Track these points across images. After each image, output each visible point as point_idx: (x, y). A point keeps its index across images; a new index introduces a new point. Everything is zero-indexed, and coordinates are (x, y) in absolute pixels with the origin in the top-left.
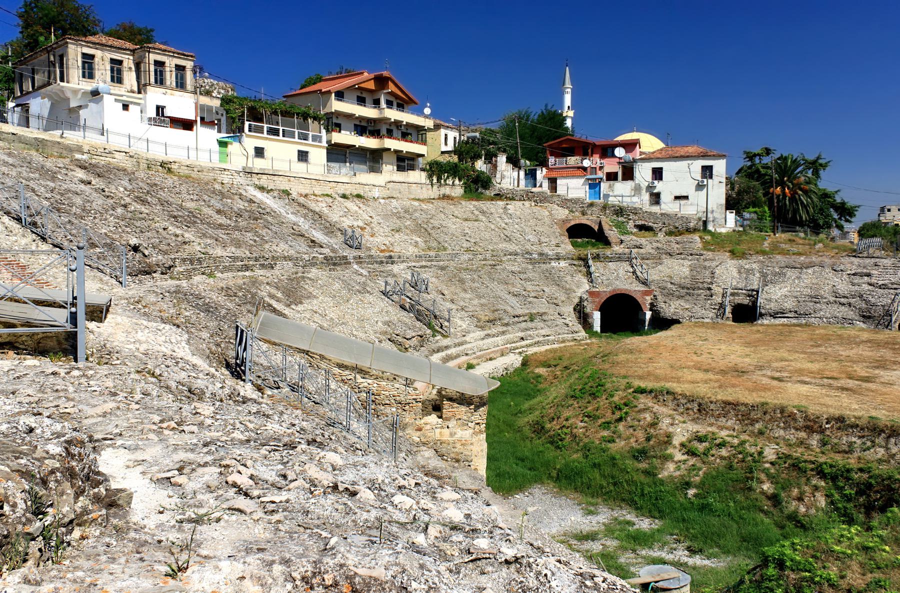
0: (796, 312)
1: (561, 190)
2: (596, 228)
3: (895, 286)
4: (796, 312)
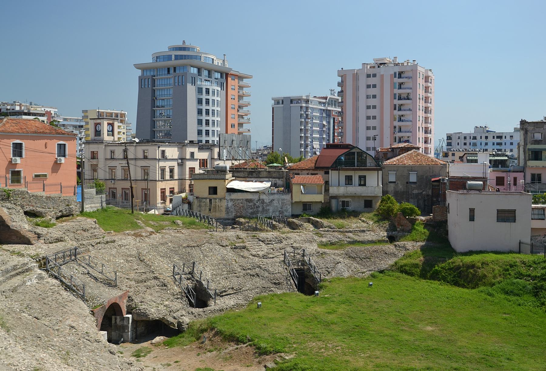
0: (233, 288)
3: (271, 256)
4: (233, 288)
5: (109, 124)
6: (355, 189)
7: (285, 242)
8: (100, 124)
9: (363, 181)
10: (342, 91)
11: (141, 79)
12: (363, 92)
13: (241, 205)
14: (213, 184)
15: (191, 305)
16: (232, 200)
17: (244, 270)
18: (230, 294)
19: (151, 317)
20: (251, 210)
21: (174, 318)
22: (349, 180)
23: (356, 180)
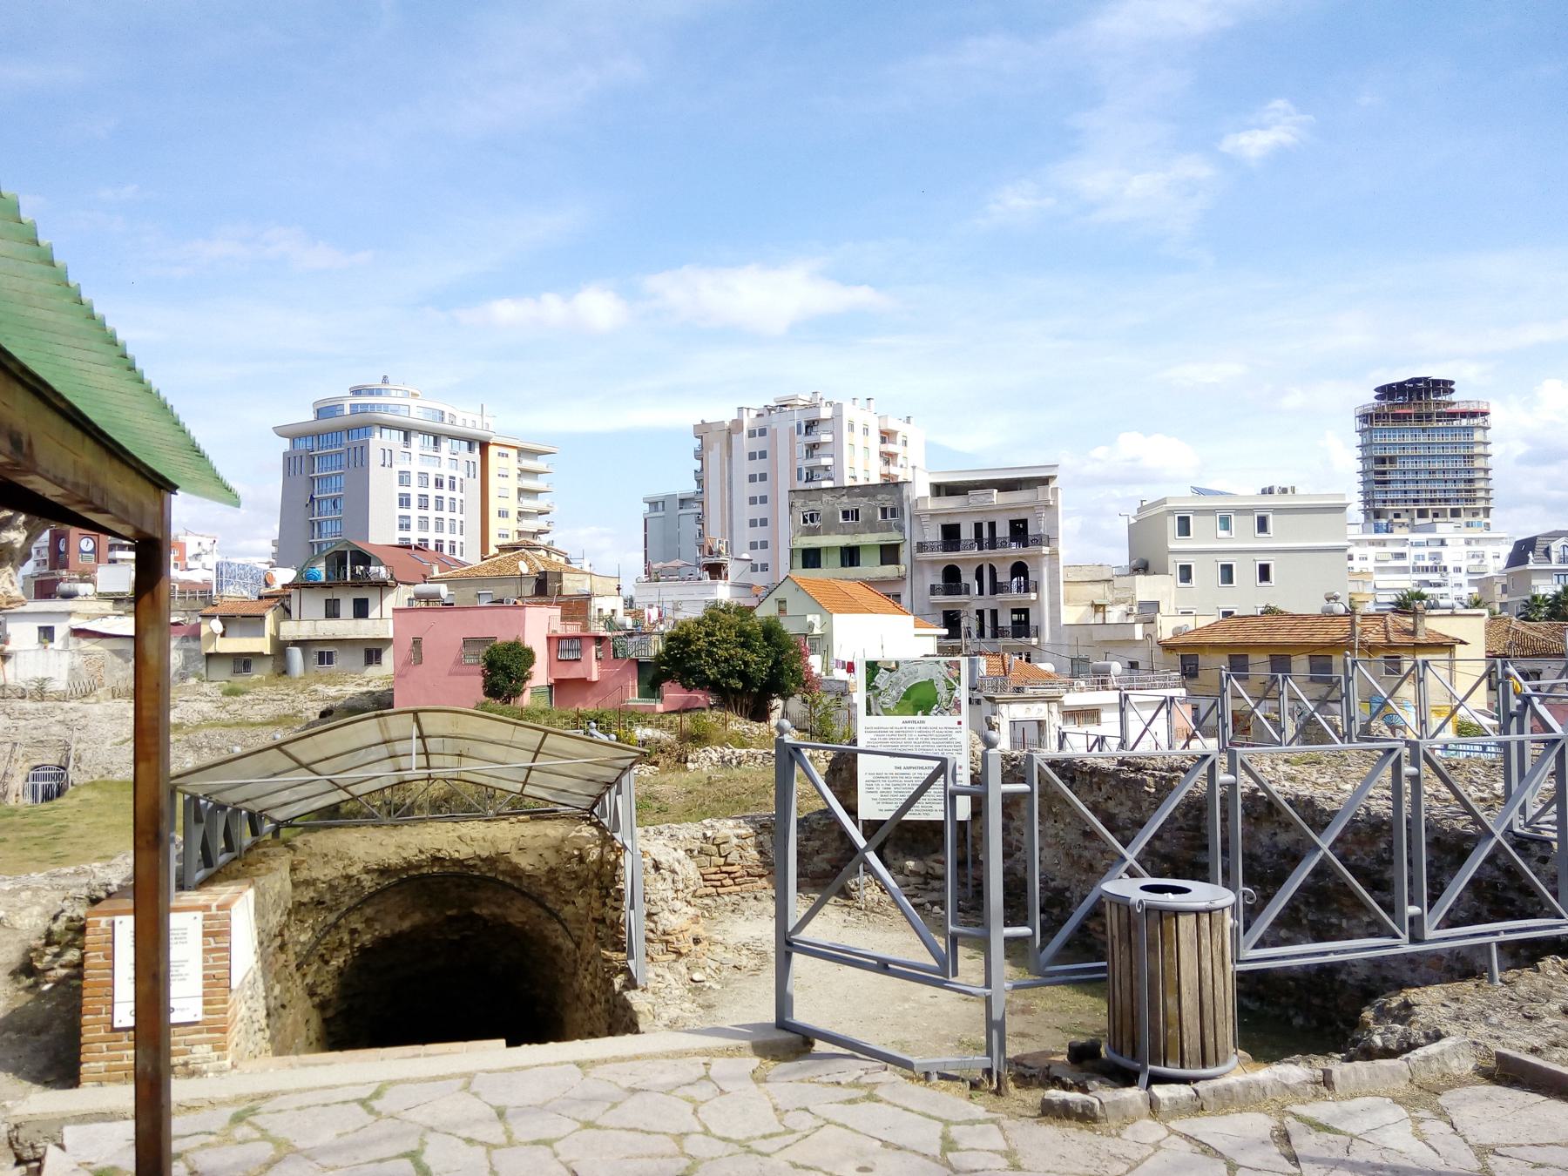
6: (346, 627)
9: (361, 610)
10: (702, 470)
11: (289, 461)
12: (744, 467)
16: (80, 652)
20: (121, 673)
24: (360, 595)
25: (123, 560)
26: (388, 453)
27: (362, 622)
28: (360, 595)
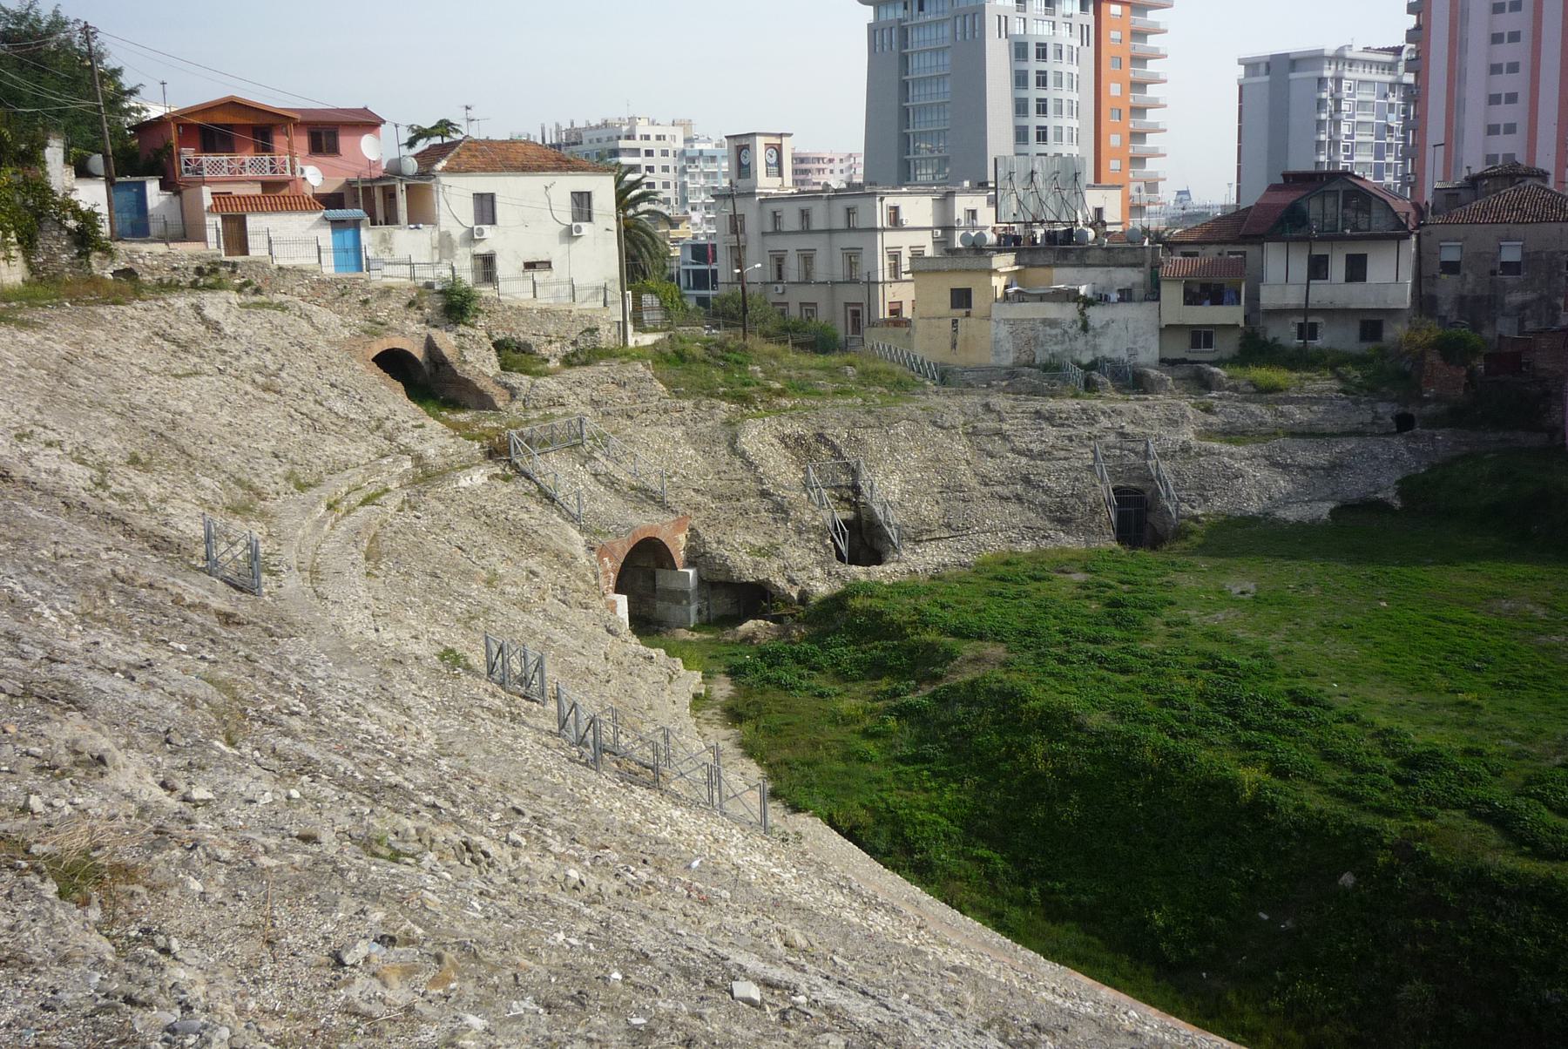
1: (257, 248)
2: (418, 352)
5: (768, 146)
6: (1335, 290)
7: (1104, 422)
8: (747, 147)
9: (1356, 271)
10: (1418, 28)
11: (873, 30)
13: (1031, 334)
14: (960, 282)
15: (840, 557)
17: (986, 485)
18: (940, 539)
19: (735, 576)
21: (791, 581)
22: (1318, 268)
23: (1338, 268)
24: (1357, 249)
25: (624, 150)
26: (1003, 19)
27: (1356, 287)
28: (1357, 249)
